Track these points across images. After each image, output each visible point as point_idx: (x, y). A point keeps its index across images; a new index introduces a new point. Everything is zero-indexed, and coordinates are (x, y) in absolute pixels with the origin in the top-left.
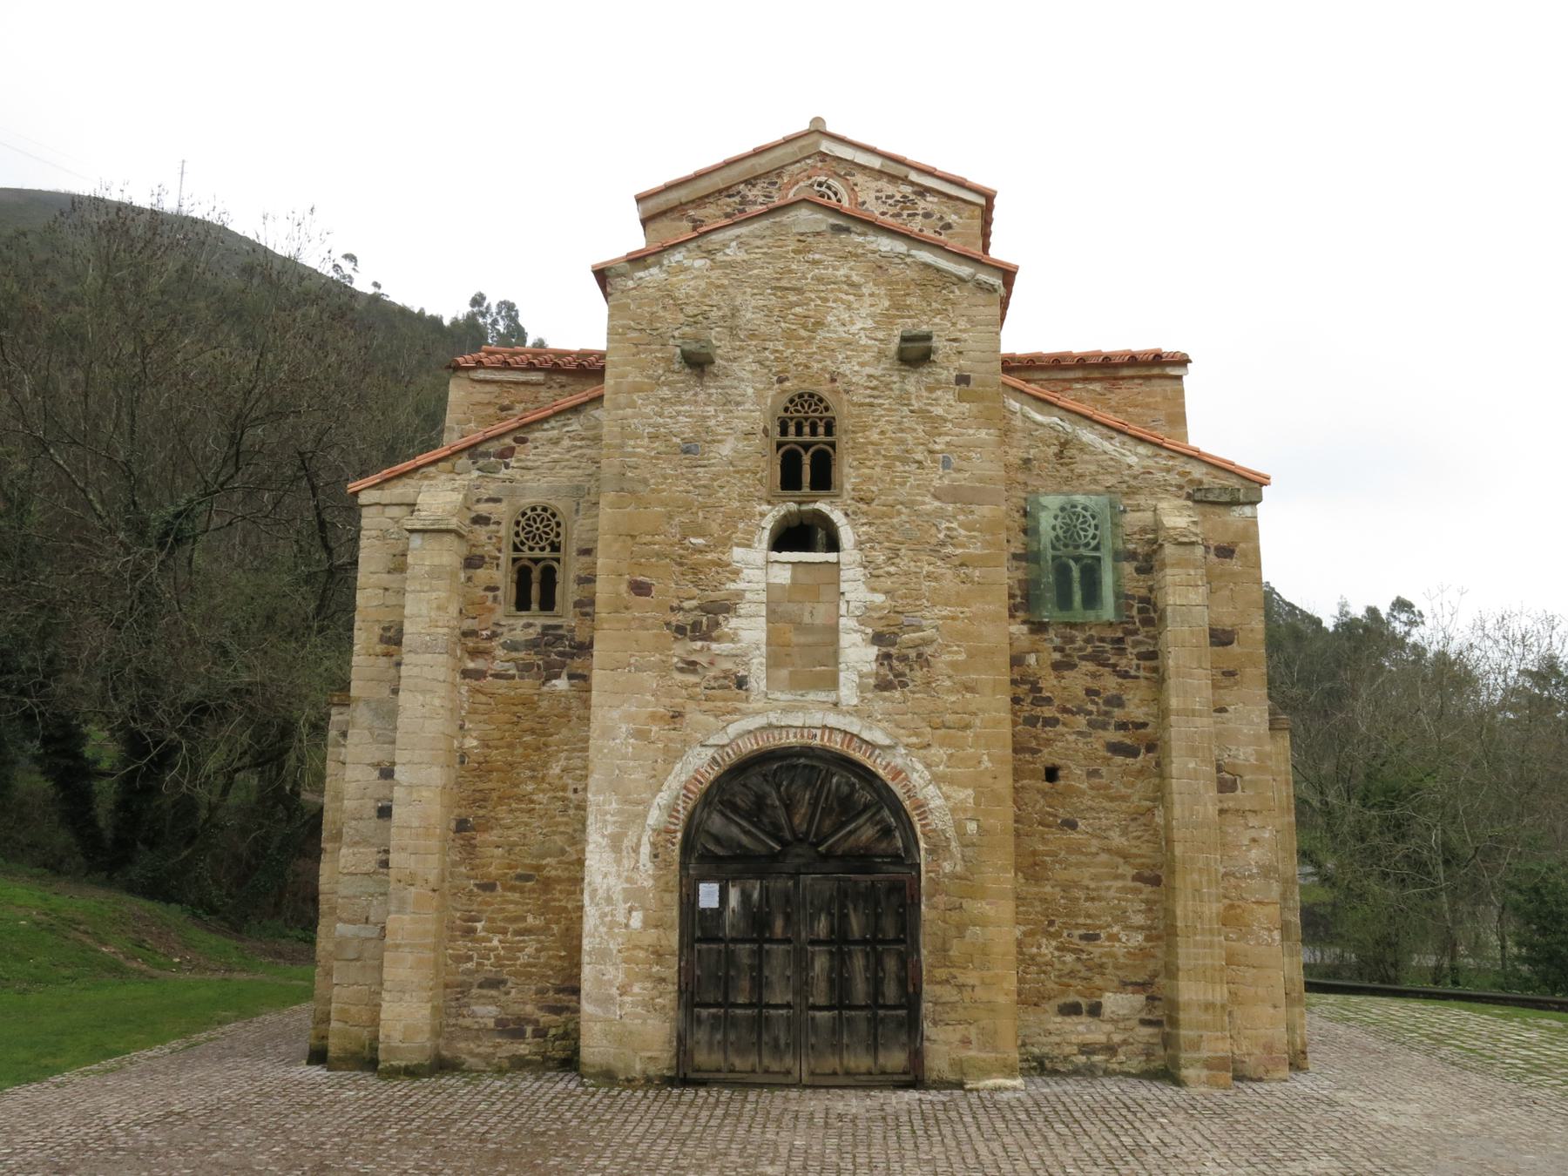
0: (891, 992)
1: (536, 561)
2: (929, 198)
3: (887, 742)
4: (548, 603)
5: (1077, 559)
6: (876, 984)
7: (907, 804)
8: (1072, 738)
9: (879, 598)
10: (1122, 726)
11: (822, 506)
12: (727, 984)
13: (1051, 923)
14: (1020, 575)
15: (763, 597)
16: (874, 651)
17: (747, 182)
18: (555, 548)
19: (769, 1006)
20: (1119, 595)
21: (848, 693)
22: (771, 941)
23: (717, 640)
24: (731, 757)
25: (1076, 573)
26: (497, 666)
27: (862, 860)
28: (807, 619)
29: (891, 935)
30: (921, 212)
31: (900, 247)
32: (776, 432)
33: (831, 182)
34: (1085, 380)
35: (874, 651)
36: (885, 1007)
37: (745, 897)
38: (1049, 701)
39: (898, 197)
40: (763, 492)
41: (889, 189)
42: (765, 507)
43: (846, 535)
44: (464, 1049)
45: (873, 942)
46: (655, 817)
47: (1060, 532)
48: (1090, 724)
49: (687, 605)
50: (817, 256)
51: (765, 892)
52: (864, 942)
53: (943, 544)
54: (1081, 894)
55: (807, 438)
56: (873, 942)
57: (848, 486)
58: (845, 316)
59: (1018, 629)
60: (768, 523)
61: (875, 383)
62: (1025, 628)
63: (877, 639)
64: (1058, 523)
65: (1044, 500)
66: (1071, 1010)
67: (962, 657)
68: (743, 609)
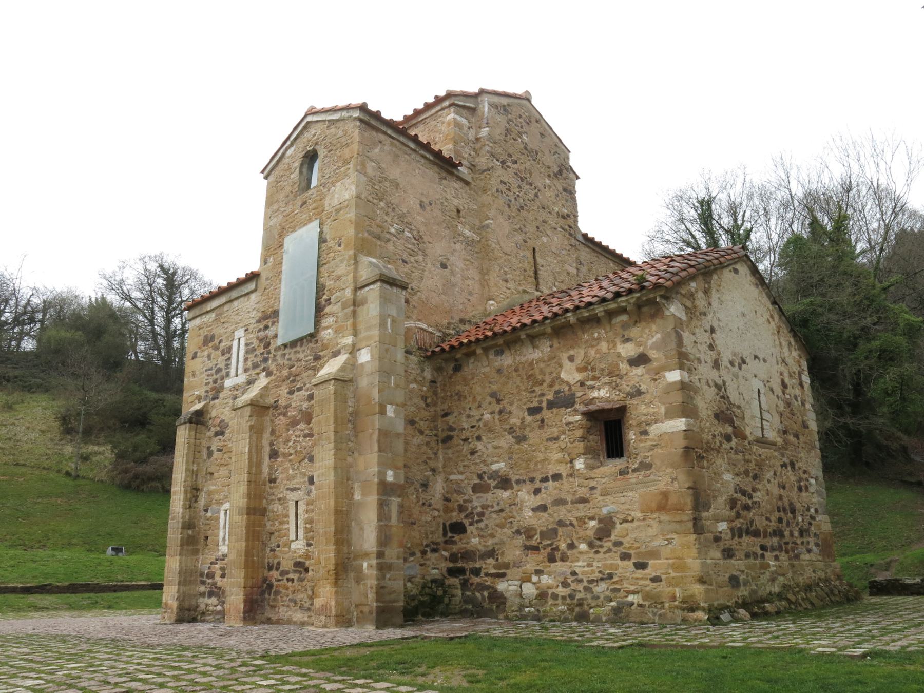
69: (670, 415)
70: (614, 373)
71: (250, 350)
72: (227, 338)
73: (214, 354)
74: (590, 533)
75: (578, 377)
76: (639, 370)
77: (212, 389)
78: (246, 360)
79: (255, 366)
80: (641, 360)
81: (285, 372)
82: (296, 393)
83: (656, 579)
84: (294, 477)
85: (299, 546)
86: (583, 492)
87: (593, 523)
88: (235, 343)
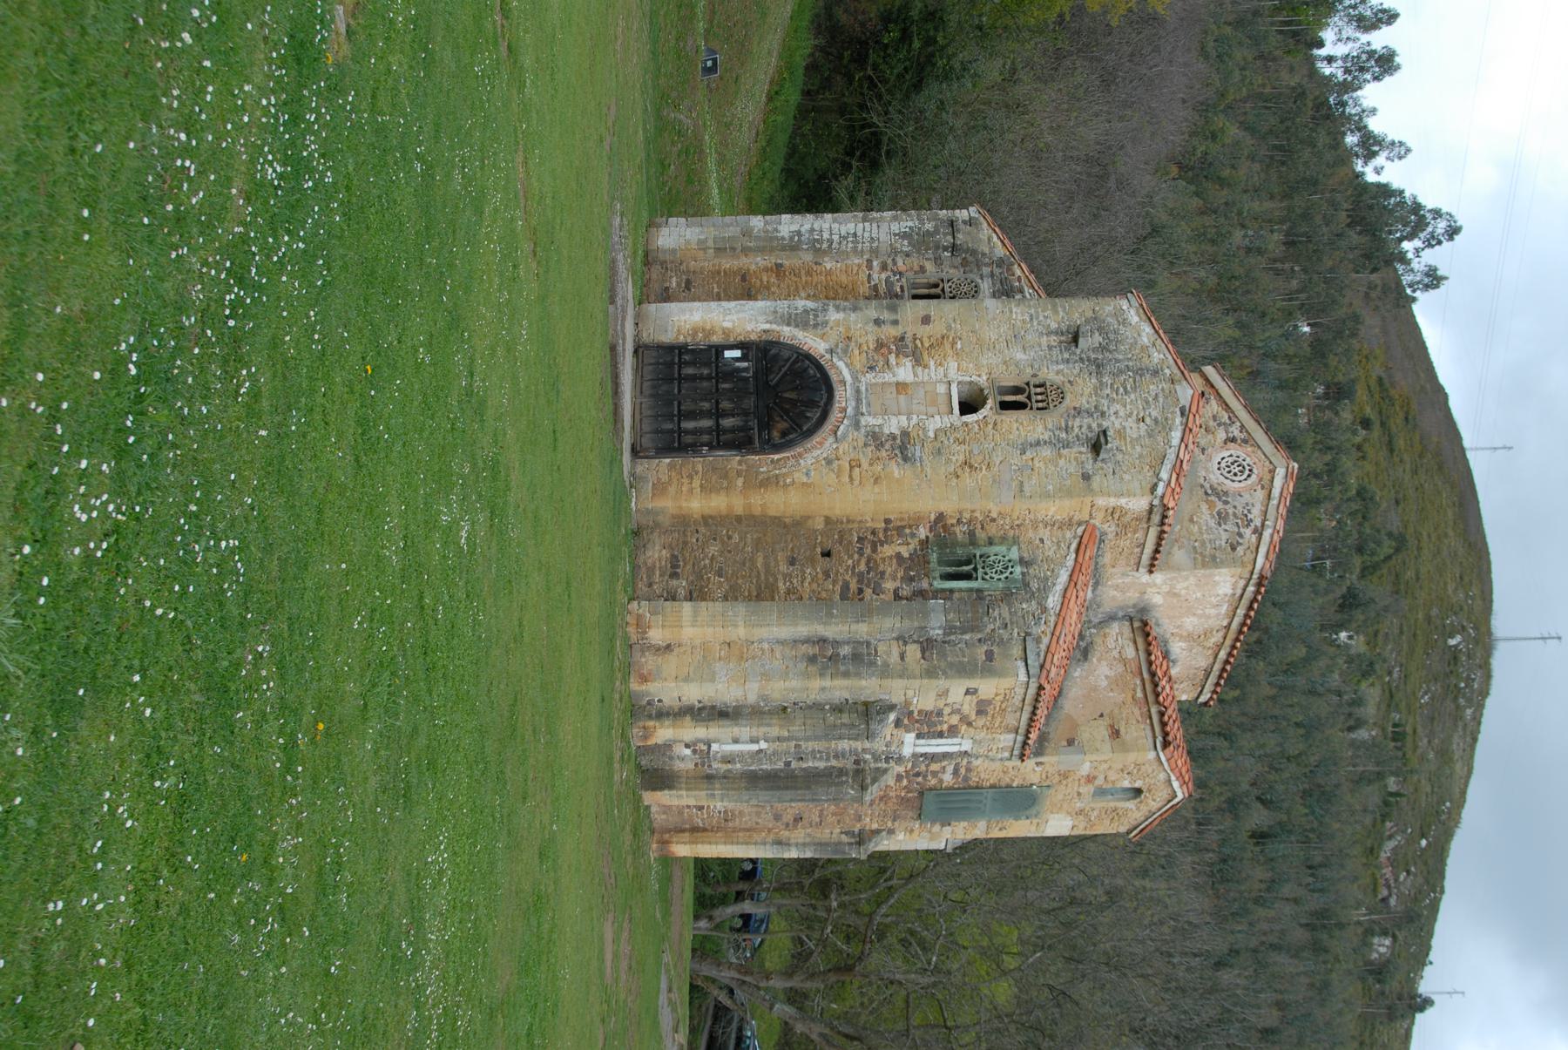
0: (688, 439)
1: (943, 290)
2: (1254, 538)
4: (915, 297)
5: (975, 569)
6: (695, 432)
7: (799, 450)
8: (850, 562)
9: (931, 434)
10: (861, 591)
11: (990, 403)
13: (730, 552)
15: (926, 378)
16: (897, 432)
17: (1242, 426)
18: (953, 297)
19: (680, 383)
20: (951, 591)
22: (717, 382)
23: (897, 356)
24: (827, 367)
25: (966, 568)
26: (875, 276)
27: (766, 425)
28: (915, 401)
29: (722, 438)
30: (1242, 530)
31: (1175, 441)
32: (1033, 381)
33: (1254, 476)
35: (897, 432)
36: (680, 436)
37: (746, 370)
38: (874, 550)
39: (1250, 516)
40: (993, 376)
42: (985, 378)
43: (970, 418)
44: (656, 272)
45: (718, 429)
47: (992, 558)
48: (861, 575)
49: (918, 342)
50: (1161, 400)
51: (747, 379)
52: (718, 425)
53: (971, 467)
55: (1034, 398)
56: (718, 429)
57: (1004, 417)
58: (1121, 413)
59: (923, 533)
60: (974, 378)
61: (1076, 430)
62: (923, 537)
63: (905, 434)
64: (999, 557)
65: (1015, 549)
67: (896, 474)
68: (920, 369)
88: (955, 741)
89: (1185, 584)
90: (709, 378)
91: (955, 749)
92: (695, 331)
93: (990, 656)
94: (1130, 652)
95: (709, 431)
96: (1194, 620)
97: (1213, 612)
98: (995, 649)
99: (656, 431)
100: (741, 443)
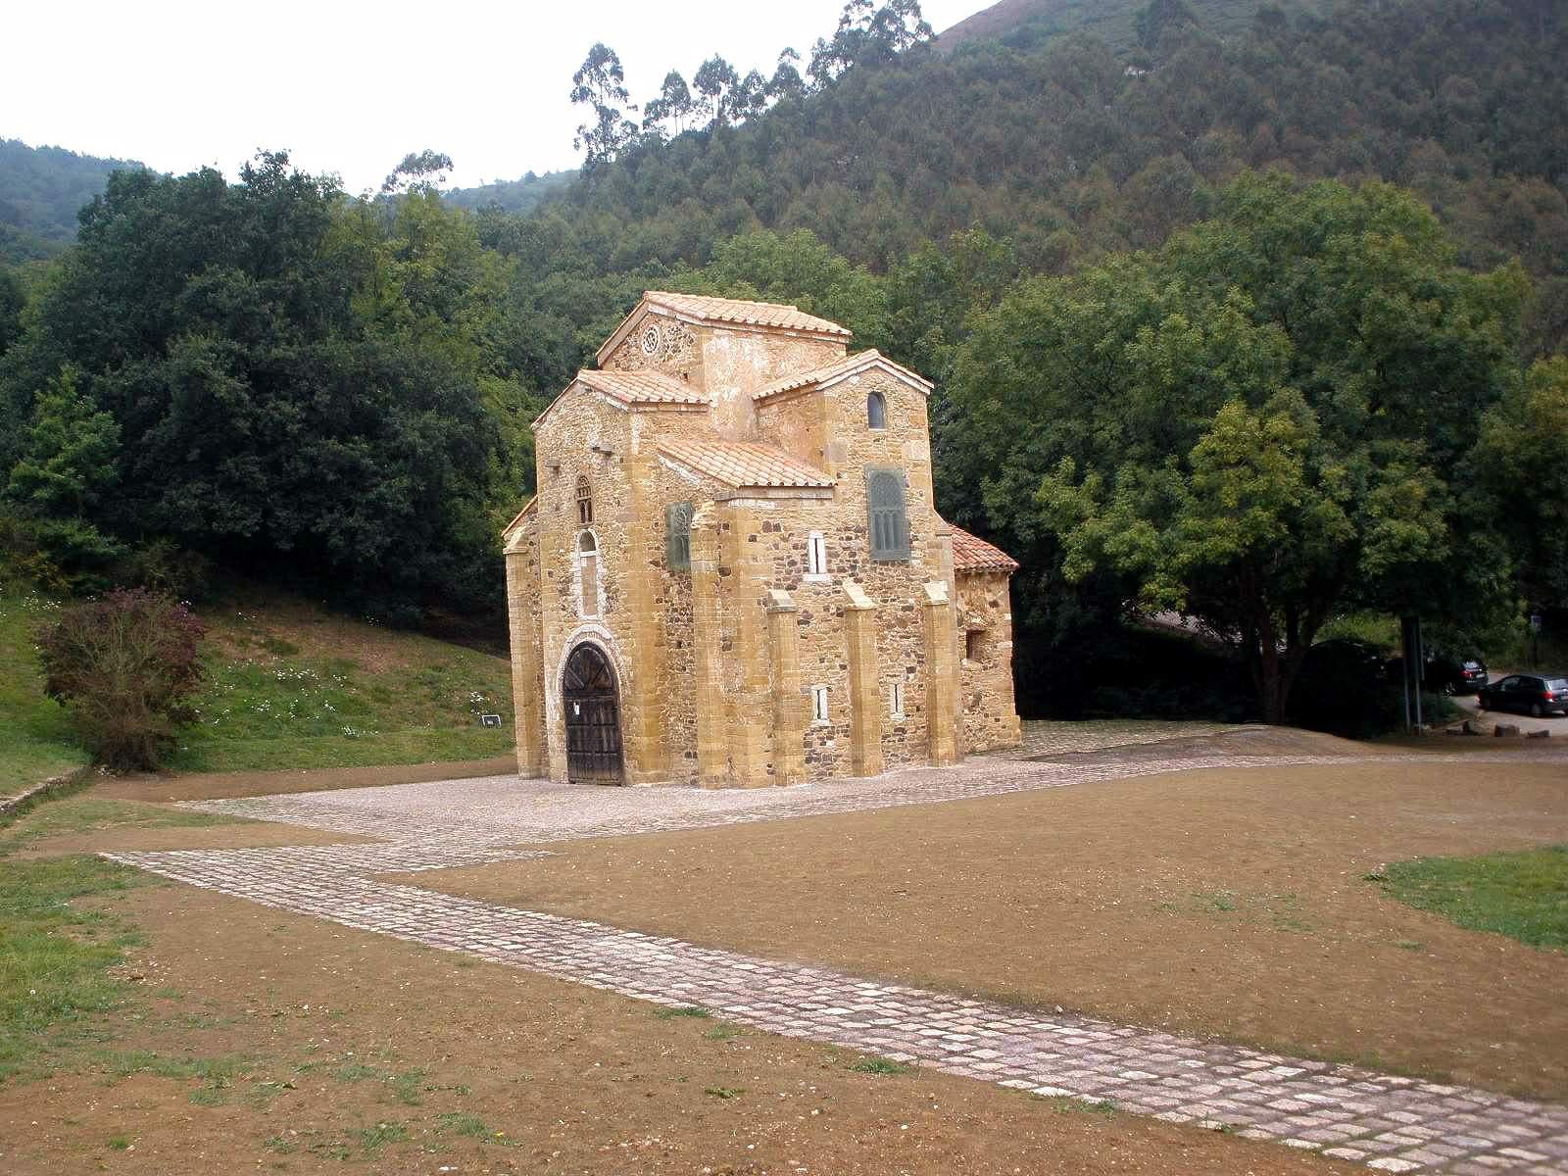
0: (612, 745)
3: (608, 636)
5: (683, 537)
6: (609, 742)
12: (576, 744)
14: (665, 548)
21: (600, 615)
34: (793, 399)
35: (605, 595)
38: (676, 610)
41: (673, 325)
46: (559, 675)
54: (687, 702)
59: (666, 575)
63: (607, 590)
66: (688, 755)
69: (1006, 638)
70: (983, 610)
71: (832, 554)
72: (800, 535)
73: (782, 544)
74: (970, 703)
75: (966, 608)
76: (994, 610)
77: (786, 579)
78: (829, 562)
79: (842, 570)
80: (994, 604)
81: (877, 583)
82: (889, 603)
83: (1004, 727)
84: (893, 667)
85: (898, 717)
86: (967, 679)
87: (971, 697)
89: (720, 373)
90: (582, 730)
91: (821, 544)
92: (560, 740)
93: (726, 527)
94: (775, 408)
95: (608, 731)
96: (755, 362)
97: (747, 348)
98: (722, 523)
99: (610, 769)
100: (612, 707)
